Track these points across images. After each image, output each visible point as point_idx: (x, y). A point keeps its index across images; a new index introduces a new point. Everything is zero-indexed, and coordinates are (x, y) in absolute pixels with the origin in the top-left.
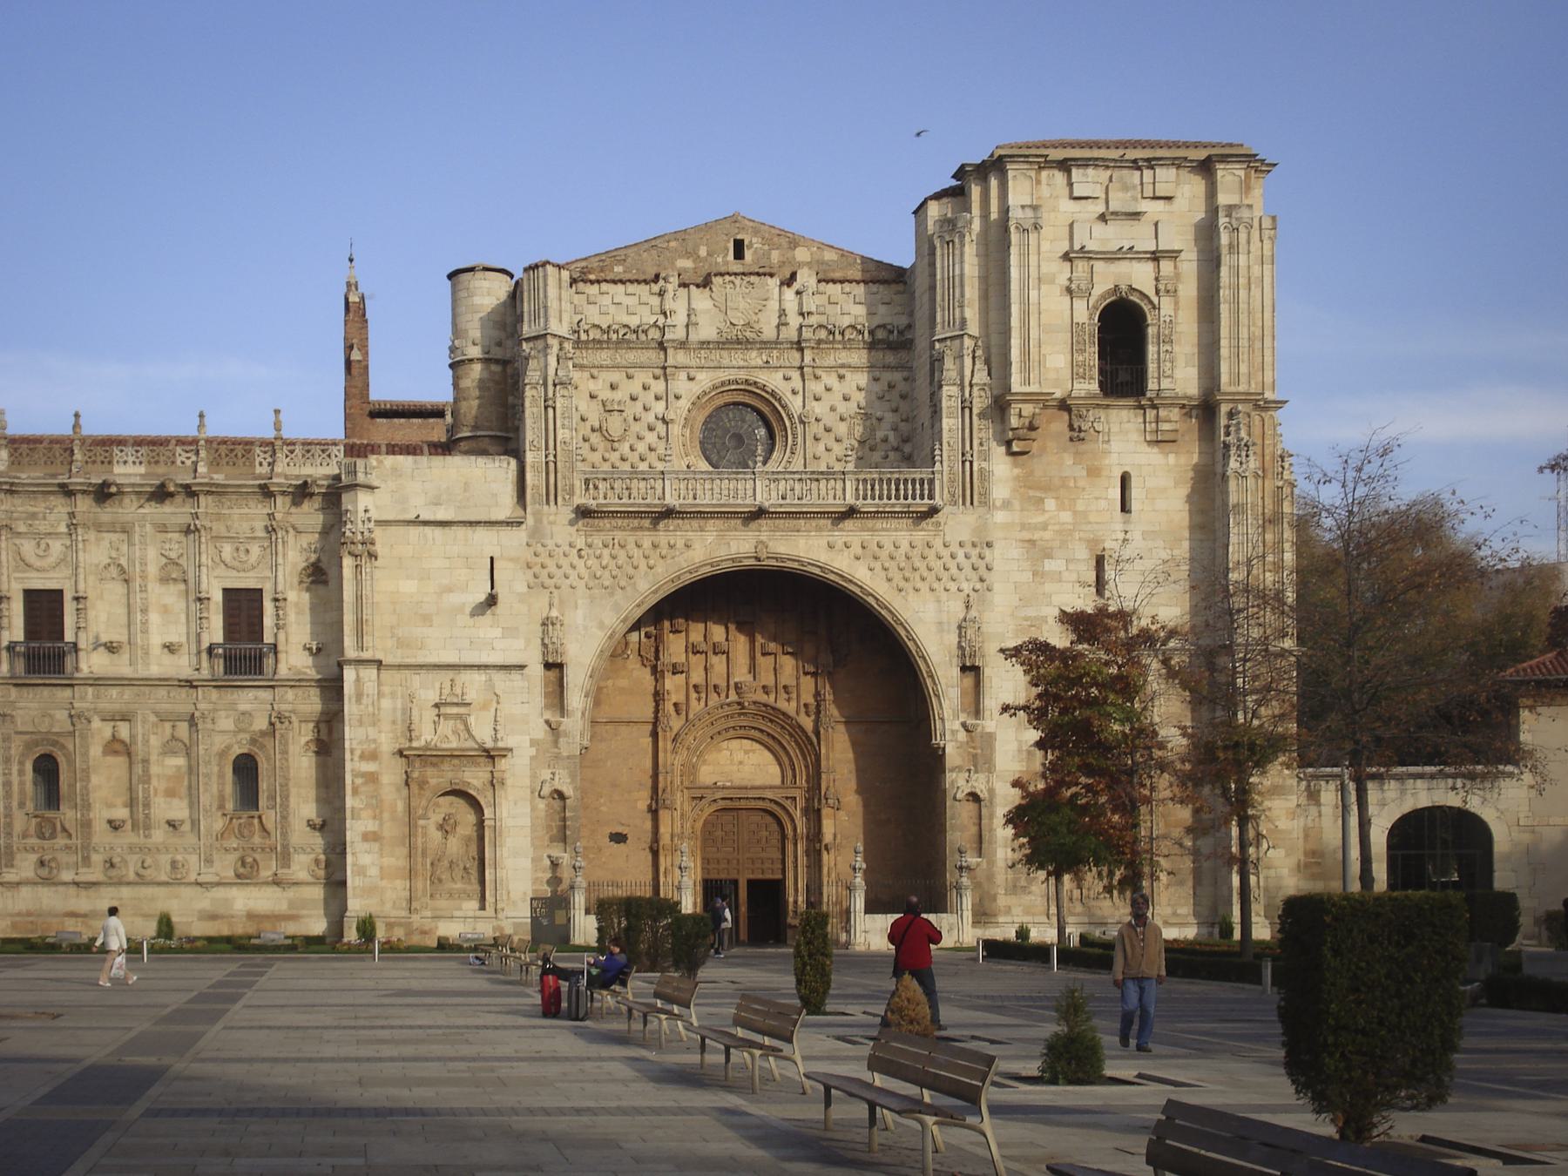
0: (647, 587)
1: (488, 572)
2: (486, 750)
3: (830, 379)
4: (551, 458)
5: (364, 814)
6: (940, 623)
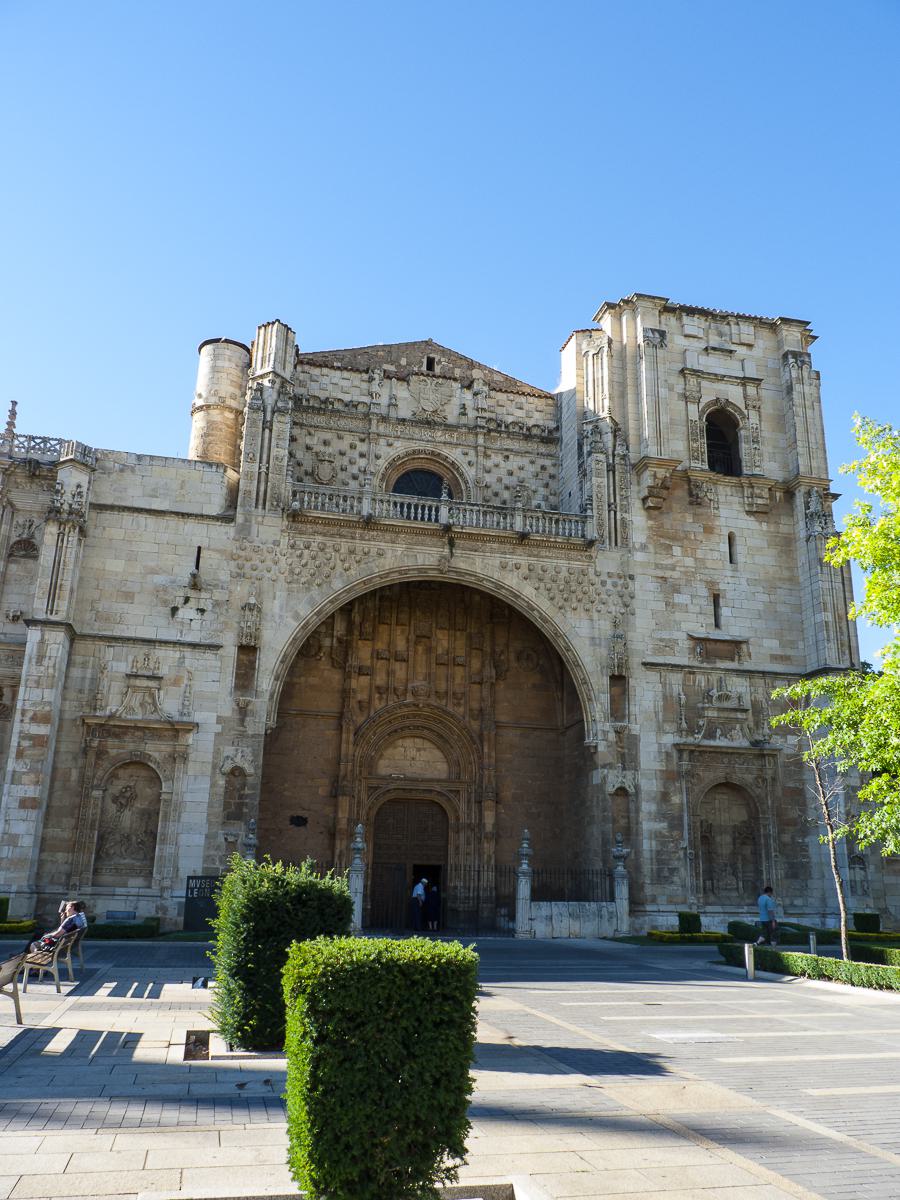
0: (341, 586)
1: (195, 560)
2: (171, 723)
3: (497, 459)
4: (264, 469)
5: (25, 779)
6: (593, 638)
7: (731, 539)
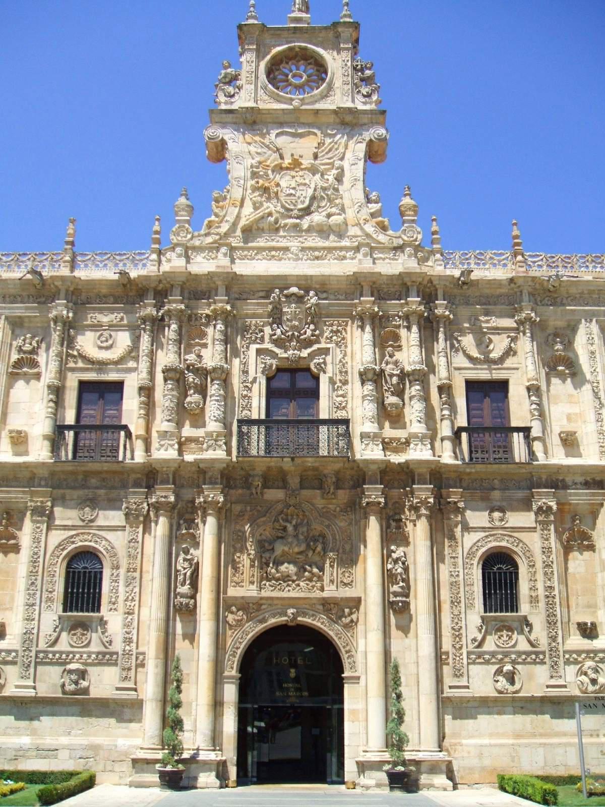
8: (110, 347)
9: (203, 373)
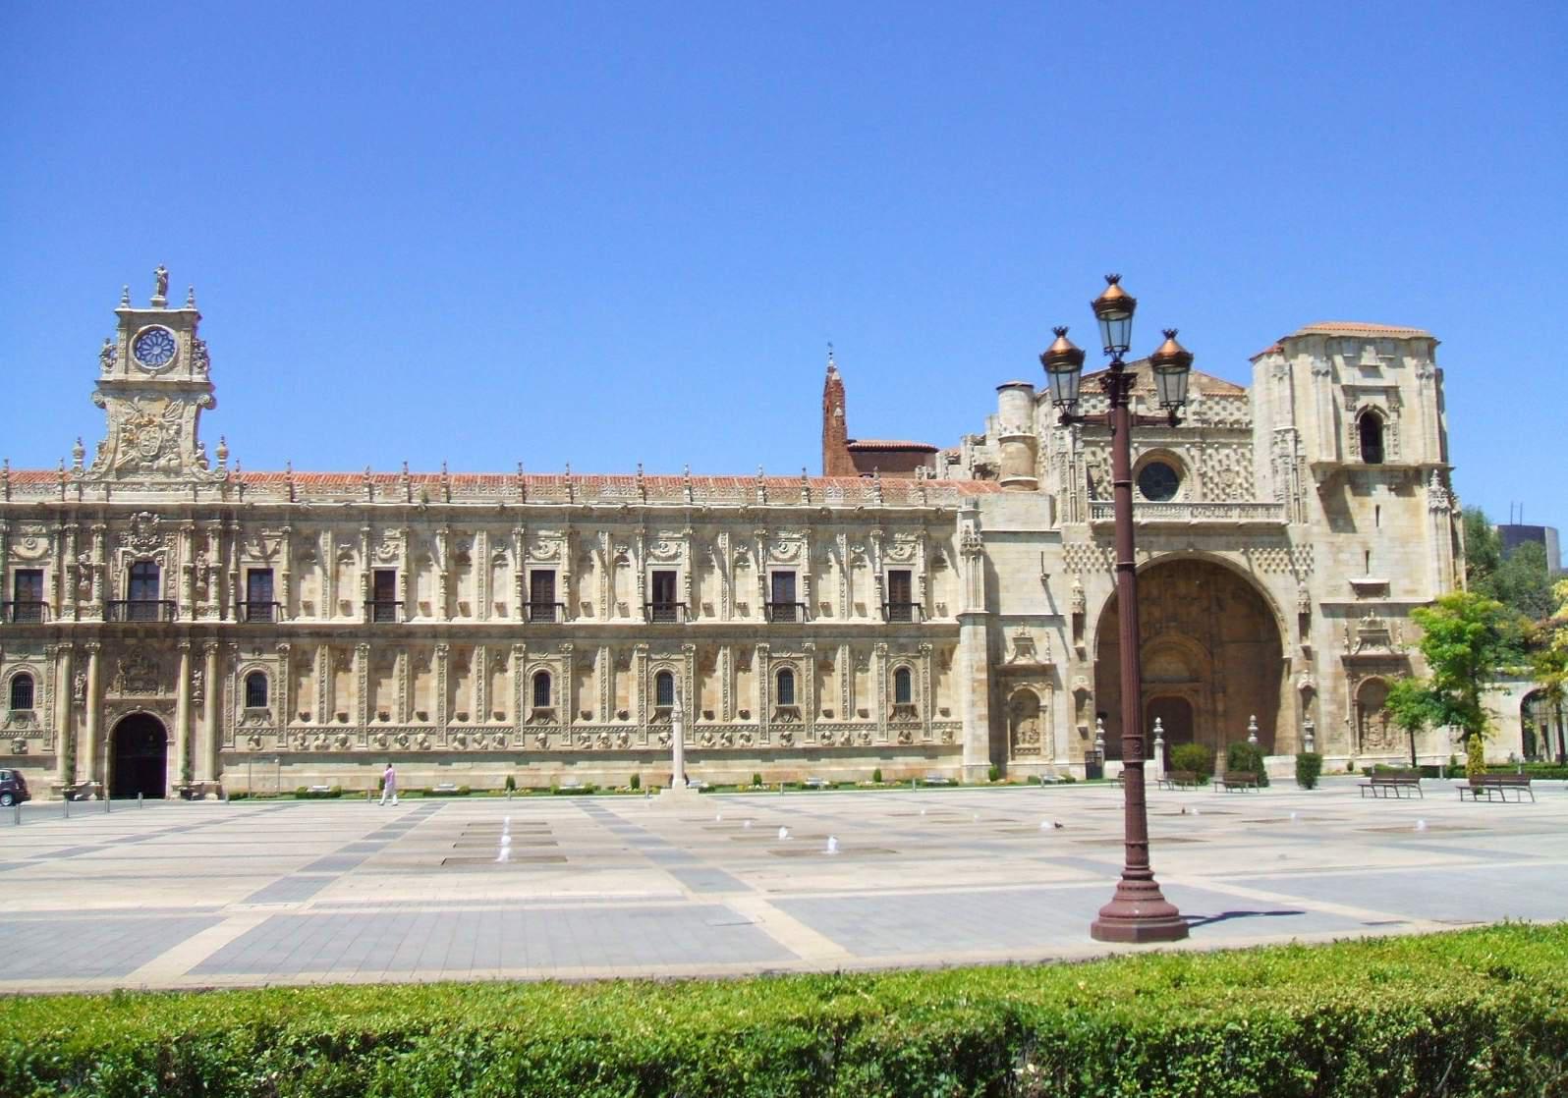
5: (979, 703)
7: (1378, 508)
8: (33, 549)
9: (89, 568)
